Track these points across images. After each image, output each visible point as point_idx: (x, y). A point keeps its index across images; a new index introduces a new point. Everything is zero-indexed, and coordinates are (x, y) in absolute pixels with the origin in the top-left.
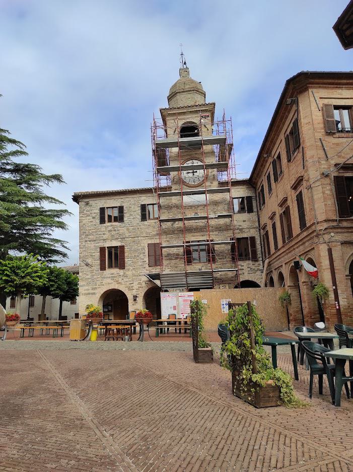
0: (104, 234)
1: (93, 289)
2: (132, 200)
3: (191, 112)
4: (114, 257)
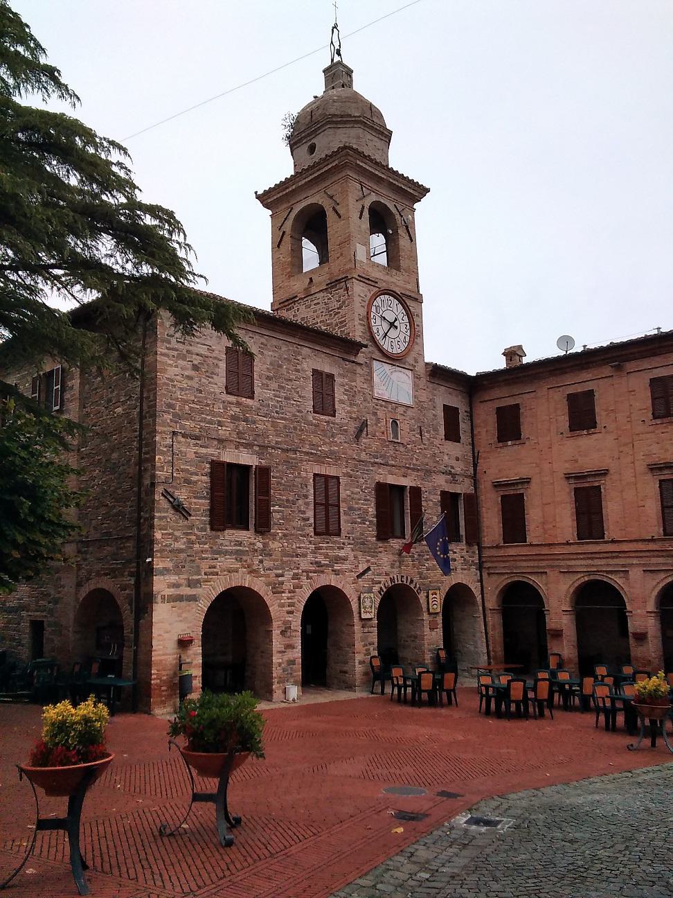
0: (220, 424)
1: (191, 584)
2: (284, 349)
4: (237, 497)
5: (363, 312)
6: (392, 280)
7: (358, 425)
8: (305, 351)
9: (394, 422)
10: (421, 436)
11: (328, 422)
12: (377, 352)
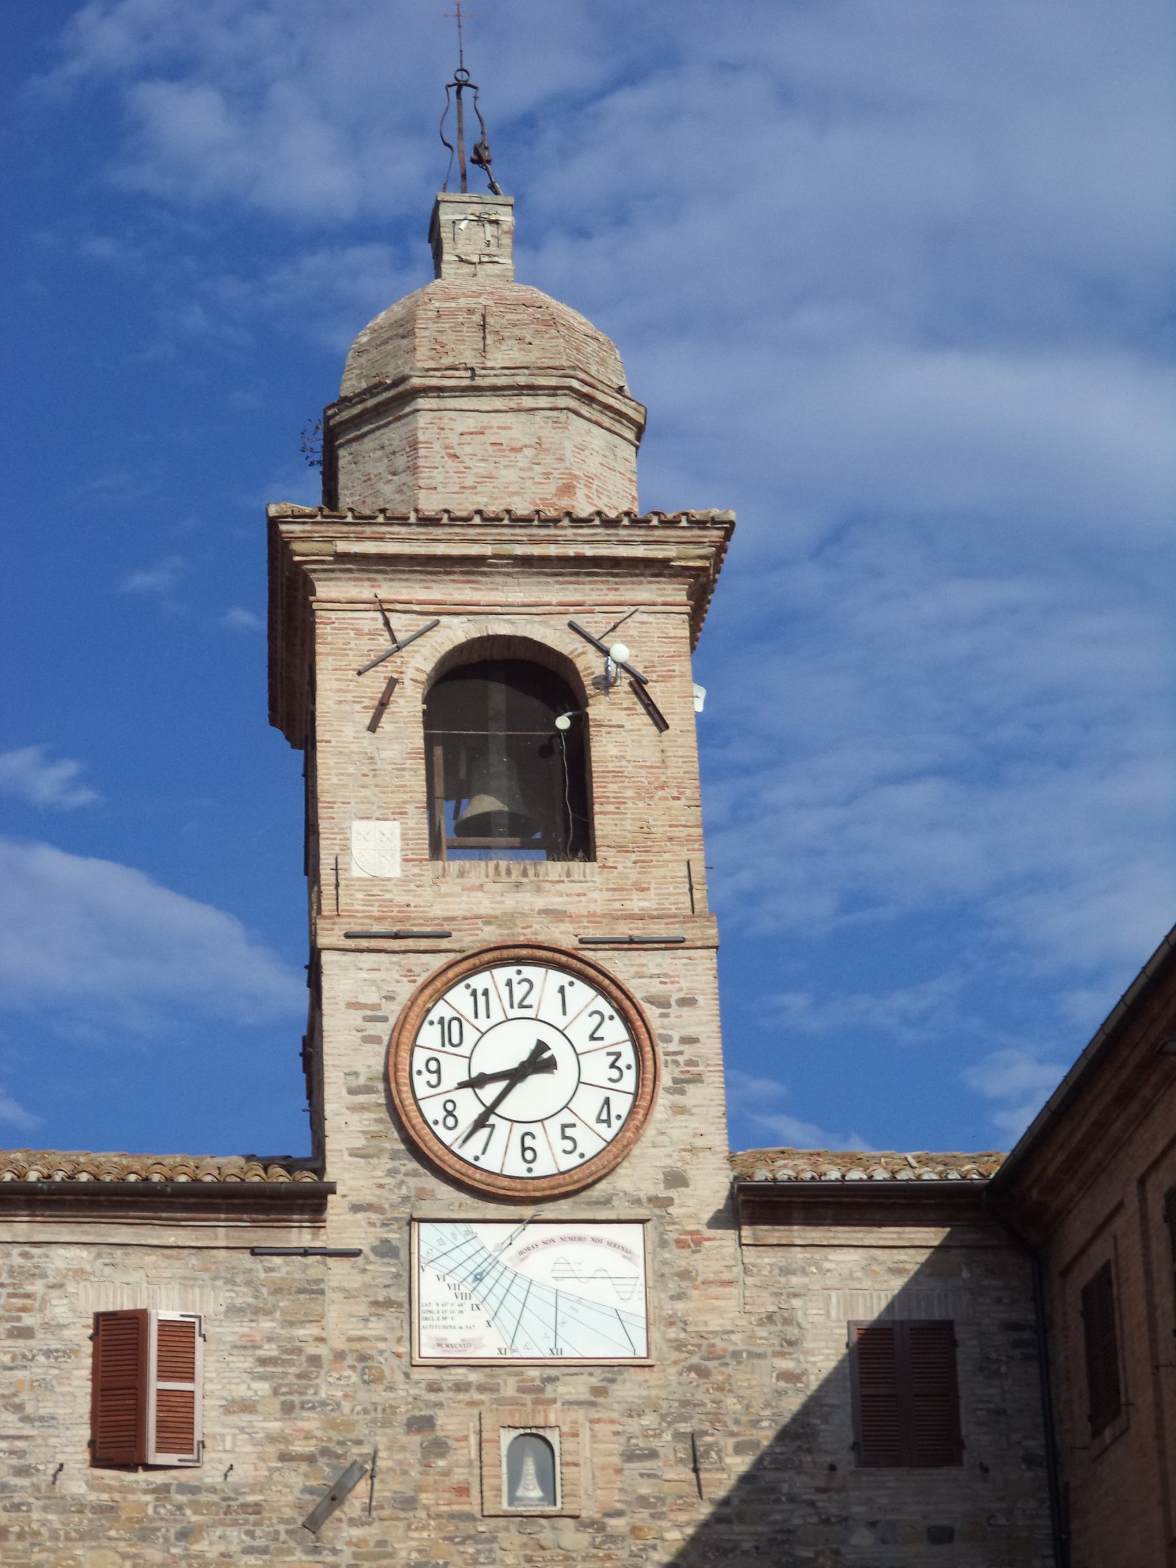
3: (527, 562)
5: (371, 1061)
6: (540, 902)
7: (326, 1474)
8: (61, 1259)
9: (534, 1438)
10: (696, 1470)
11: (162, 1491)
12: (446, 1192)
